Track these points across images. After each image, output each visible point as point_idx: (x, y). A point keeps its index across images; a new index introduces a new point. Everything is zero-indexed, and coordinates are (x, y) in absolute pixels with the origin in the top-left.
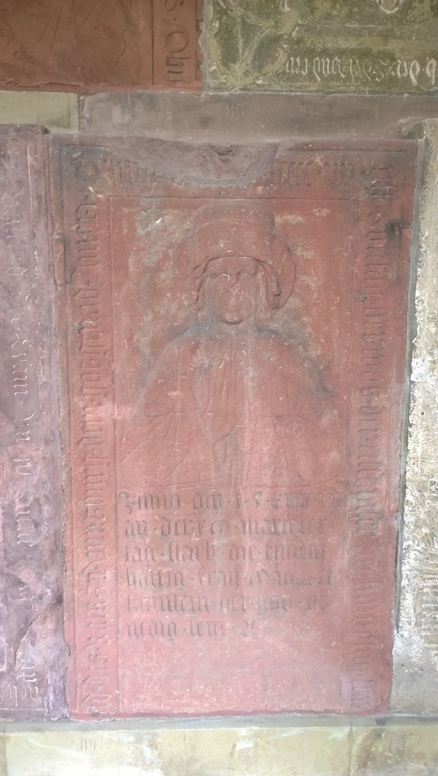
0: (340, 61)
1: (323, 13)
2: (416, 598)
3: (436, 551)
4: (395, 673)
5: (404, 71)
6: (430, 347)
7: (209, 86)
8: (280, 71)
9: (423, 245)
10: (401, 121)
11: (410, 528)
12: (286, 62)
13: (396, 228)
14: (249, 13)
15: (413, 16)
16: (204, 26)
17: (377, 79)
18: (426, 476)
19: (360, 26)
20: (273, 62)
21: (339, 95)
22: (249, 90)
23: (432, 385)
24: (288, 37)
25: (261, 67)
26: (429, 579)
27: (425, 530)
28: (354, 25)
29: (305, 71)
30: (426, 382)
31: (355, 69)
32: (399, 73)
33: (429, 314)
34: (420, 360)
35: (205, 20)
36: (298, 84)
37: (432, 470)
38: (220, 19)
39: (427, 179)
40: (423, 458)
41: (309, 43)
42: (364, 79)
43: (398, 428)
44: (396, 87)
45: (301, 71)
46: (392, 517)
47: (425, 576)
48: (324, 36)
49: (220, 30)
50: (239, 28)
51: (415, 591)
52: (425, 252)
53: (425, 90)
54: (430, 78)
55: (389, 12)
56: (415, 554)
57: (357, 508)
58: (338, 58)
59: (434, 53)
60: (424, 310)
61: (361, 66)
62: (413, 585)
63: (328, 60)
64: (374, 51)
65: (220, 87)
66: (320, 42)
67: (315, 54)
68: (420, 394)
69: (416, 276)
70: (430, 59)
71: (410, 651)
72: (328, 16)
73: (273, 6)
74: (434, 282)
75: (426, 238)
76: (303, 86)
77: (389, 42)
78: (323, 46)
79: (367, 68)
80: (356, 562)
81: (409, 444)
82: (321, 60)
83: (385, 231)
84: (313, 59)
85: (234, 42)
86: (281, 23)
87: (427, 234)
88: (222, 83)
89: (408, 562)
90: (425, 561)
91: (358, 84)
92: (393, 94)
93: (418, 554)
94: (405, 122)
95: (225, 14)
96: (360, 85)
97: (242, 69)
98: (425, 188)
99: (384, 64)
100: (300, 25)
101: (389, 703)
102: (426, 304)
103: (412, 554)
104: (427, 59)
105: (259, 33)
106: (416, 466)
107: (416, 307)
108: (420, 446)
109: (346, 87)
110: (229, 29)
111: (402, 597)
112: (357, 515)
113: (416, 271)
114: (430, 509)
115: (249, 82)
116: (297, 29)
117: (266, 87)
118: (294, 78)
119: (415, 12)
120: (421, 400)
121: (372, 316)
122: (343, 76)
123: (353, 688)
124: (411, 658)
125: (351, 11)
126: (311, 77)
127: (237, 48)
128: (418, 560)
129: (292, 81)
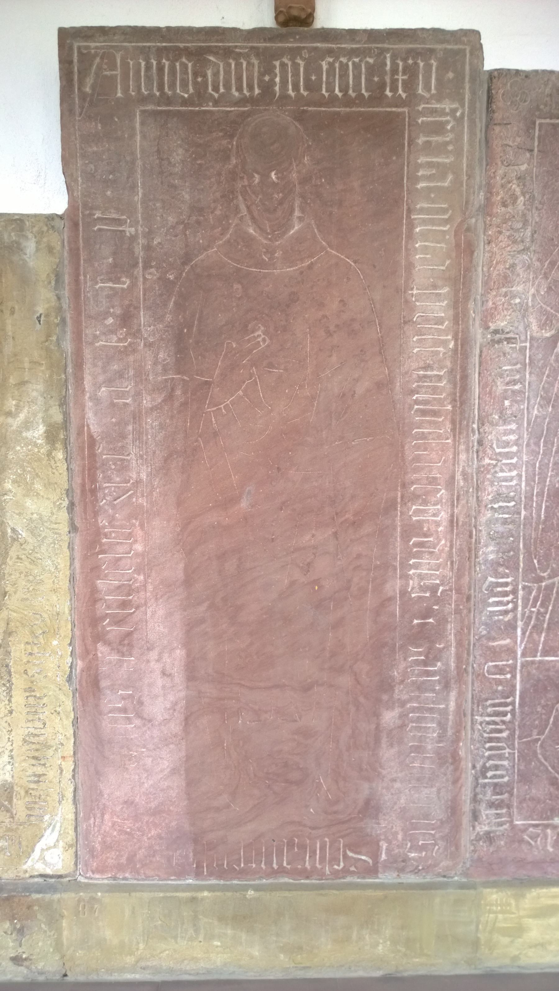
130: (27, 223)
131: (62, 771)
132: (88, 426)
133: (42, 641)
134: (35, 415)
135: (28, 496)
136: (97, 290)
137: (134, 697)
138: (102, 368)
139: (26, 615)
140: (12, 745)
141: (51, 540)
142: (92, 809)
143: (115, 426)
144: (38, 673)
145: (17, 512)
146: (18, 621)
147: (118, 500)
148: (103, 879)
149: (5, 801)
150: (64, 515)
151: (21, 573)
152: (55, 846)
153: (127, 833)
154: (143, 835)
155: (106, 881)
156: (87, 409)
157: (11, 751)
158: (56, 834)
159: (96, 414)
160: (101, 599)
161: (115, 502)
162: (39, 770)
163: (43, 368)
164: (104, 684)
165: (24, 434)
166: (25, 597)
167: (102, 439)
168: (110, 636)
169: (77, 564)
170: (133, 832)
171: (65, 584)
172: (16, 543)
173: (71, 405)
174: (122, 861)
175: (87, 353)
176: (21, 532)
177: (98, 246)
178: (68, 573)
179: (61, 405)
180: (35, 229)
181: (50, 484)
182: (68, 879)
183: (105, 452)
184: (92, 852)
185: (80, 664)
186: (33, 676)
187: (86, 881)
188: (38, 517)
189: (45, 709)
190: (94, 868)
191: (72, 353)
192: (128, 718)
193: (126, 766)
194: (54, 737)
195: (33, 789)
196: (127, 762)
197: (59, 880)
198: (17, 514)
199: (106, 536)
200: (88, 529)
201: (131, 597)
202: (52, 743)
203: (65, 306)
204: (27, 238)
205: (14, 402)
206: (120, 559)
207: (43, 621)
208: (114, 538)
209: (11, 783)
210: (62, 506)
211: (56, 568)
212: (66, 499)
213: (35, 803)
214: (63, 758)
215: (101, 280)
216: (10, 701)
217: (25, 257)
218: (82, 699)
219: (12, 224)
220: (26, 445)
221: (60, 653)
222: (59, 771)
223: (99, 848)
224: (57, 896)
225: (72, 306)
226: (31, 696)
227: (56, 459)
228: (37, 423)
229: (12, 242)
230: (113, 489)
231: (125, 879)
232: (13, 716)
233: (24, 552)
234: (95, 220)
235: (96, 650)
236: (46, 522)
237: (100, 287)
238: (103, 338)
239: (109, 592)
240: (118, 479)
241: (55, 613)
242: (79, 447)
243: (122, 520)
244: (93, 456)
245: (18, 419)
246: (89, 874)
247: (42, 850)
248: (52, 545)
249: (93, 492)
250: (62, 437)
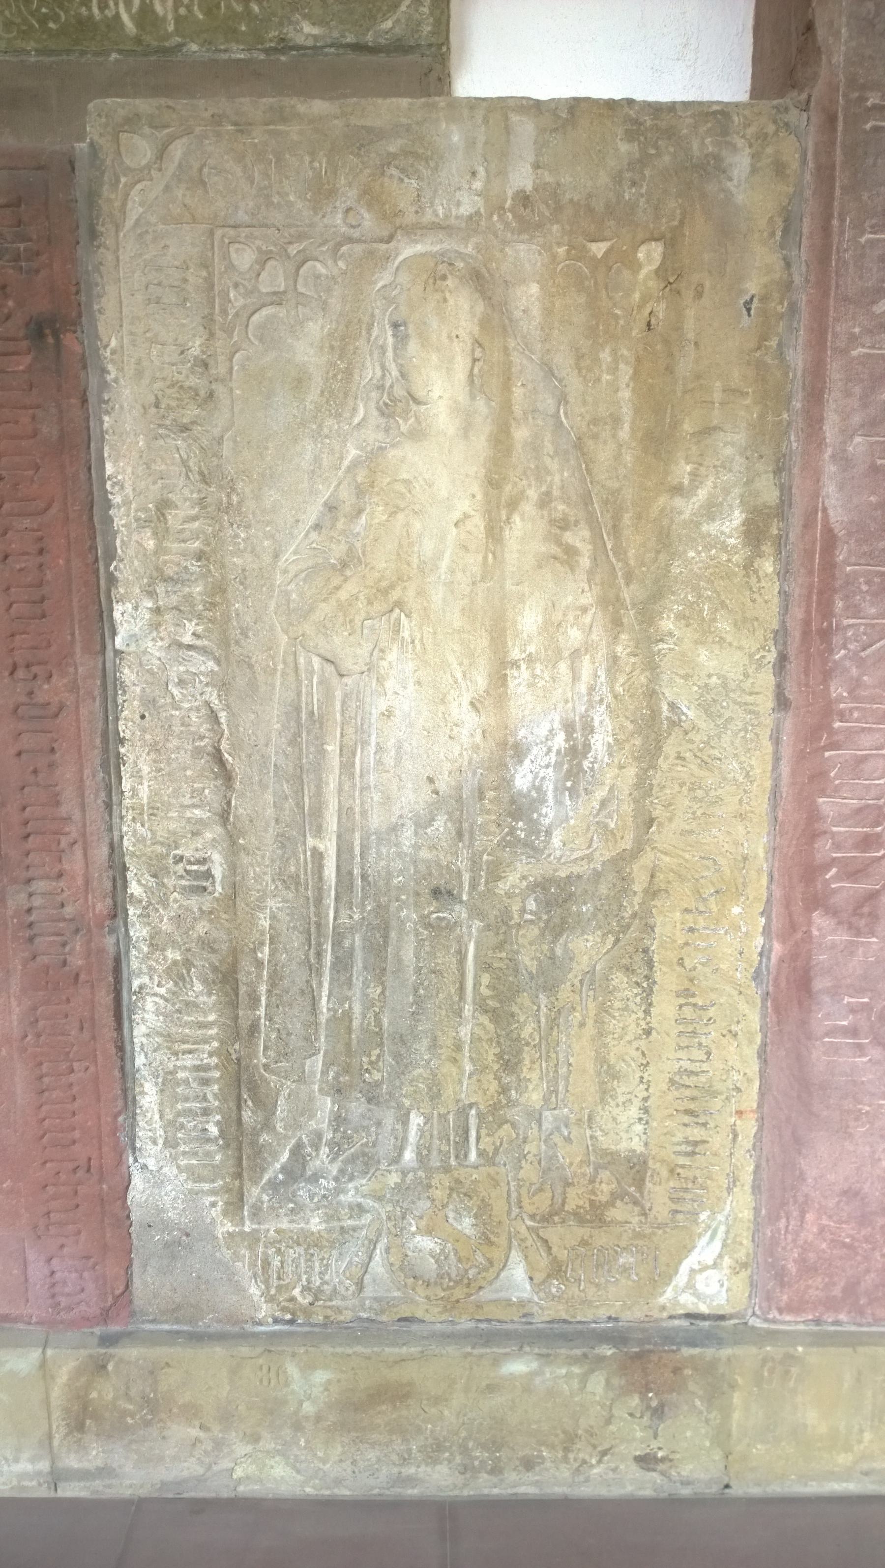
2: (162, 1091)
3: (197, 997)
4: (135, 1242)
6: (145, 581)
9: (110, 367)
11: (139, 950)
13: (47, 331)
17: (51, 25)
18: (162, 844)
23: (160, 659)
26: (184, 1053)
27: (172, 955)
30: (145, 652)
32: (96, 11)
33: (136, 511)
34: (129, 606)
37: (175, 833)
39: (100, 228)
40: (153, 808)
43: (94, 747)
46: (103, 927)
47: (176, 1047)
51: (158, 1076)
52: (116, 380)
53: (155, 44)
54: (164, 19)
56: (156, 1003)
57: (29, 911)
60: (127, 503)
62: (154, 1064)
68: (133, 677)
69: (102, 431)
71: (161, 1196)
74: (141, 443)
75: (114, 352)
80: (37, 1021)
81: (124, 781)
83: (26, 337)
87: (113, 343)
89: (143, 1019)
90: (176, 1016)
91: (11, 36)
93: (161, 1002)
96: (15, 38)
98: (98, 247)
101: (131, 1301)
102: (129, 490)
103: (150, 1004)
106: (139, 824)
107: (110, 497)
108: (146, 784)
111: (137, 1090)
112: (30, 925)
113: (102, 422)
114: (180, 912)
120: (138, 689)
121: (19, 515)
123: (53, 1273)
124: (162, 1211)
128: (162, 1014)
130: (736, 119)
131: (735, 1136)
132: (825, 510)
133: (715, 908)
134: (726, 491)
135: (702, 643)
136: (863, 247)
137: (872, 1009)
138: (861, 398)
139: (687, 861)
140: (647, 1090)
141: (740, 725)
142: (784, 1204)
143: (876, 509)
144: (703, 964)
145: (682, 672)
146: (672, 870)
147: (869, 651)
148: (797, 1323)
149: (630, 1186)
150: (767, 679)
151: (682, 785)
152: (715, 1265)
153: (844, 1245)
154: (873, 1249)
155: (801, 1327)
156: (825, 479)
157: (645, 1099)
158: (717, 1245)
159: (841, 488)
160: (825, 832)
161: (863, 654)
162: (696, 1133)
163: (748, 401)
164: (820, 984)
165: (705, 528)
166: (687, 827)
167: (849, 534)
168: (837, 900)
169: (785, 769)
170: (856, 1244)
171: (761, 805)
172: (676, 729)
173: (796, 471)
174: (834, 1293)
175: (835, 371)
176: (685, 710)
177: (870, 161)
178: (768, 784)
179: (778, 472)
180: (750, 131)
181: (745, 620)
182: (732, 1322)
183: (853, 560)
184: (781, 1277)
185: (777, 948)
186: (695, 969)
187: (765, 1325)
188: (719, 682)
189: (711, 1028)
190: (782, 1304)
191: (804, 370)
192: (859, 1046)
193: (849, 1130)
194: (724, 1077)
195: (683, 1167)
196: (852, 1123)
197: (718, 1323)
198: (682, 677)
199: (842, 718)
200: (811, 704)
201: (879, 829)
202: (718, 1086)
203: (797, 279)
204: (734, 148)
205: (688, 468)
206: (865, 758)
207: (717, 871)
208: (857, 721)
209: (642, 1154)
210: (766, 661)
211: (747, 775)
212: (773, 649)
213: (686, 1190)
214: (740, 1113)
215: (872, 227)
216: (647, 1012)
217: (729, 184)
218: (777, 1010)
219: (707, 122)
220: (708, 547)
221: (744, 929)
222: (731, 1136)
223: (794, 1270)
224: (726, 1352)
225: (812, 278)
226: (687, 1004)
227: (761, 573)
228: (730, 506)
229: (707, 155)
230: (862, 628)
231: (837, 1323)
232: (651, 1038)
233: (691, 746)
234: (870, 109)
235: (810, 923)
236: (734, 691)
237: (869, 241)
238: (867, 340)
239: (841, 819)
240: (873, 611)
241: (740, 858)
242: (805, 550)
243: (874, 687)
244: (829, 566)
245: (695, 499)
246: (774, 1314)
247: (693, 1271)
248: (742, 734)
249: (825, 635)
250: (776, 532)
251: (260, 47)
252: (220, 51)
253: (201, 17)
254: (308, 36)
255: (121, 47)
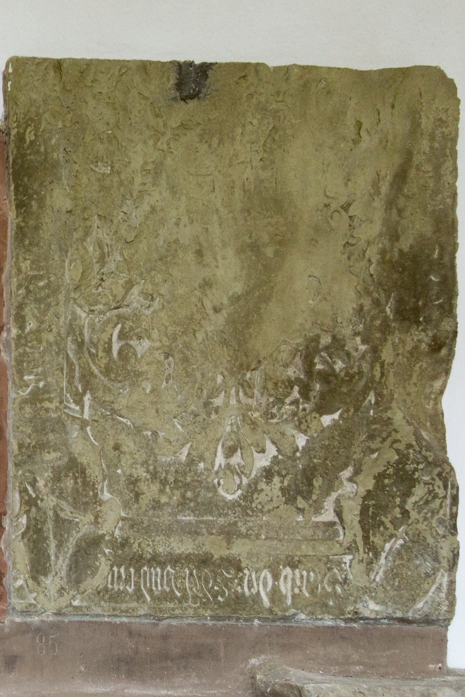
0: (173, 571)
1: (150, 500)
5: (252, 586)
7: (14, 609)
8: (101, 587)
10: (254, 661)
12: (109, 573)
14: (62, 502)
15: (260, 503)
16: (8, 521)
17: (220, 598)
19: (196, 518)
20: (93, 574)
21: (174, 622)
22: (64, 614)
24: (110, 538)
25: (78, 582)
28: (188, 518)
29: (130, 587)
31: (192, 584)
32: (246, 589)
35: (9, 512)
36: (124, 606)
38: (28, 512)
41: (136, 545)
42: (204, 598)
44: (244, 609)
45: (126, 585)
48: (154, 534)
49: (28, 528)
50: (50, 525)
53: (280, 613)
54: (286, 597)
55: (229, 497)
58: (171, 568)
59: (289, 559)
61: (200, 578)
63: (159, 570)
64: (216, 557)
65: (28, 610)
66: (149, 545)
67: (143, 561)
70: (284, 567)
72: (157, 505)
73: (91, 493)
76: (130, 608)
77: (233, 543)
78: (153, 551)
79: (207, 582)
82: (150, 571)
84: (141, 568)
85: (45, 545)
86: (101, 518)
88: (30, 605)
91: (196, 606)
92: (240, 619)
94: (257, 664)
95: (35, 506)
96: (199, 608)
97: (56, 585)
99: (228, 576)
100: (123, 519)
104: (281, 567)
105: (74, 532)
109: (182, 610)
110: (39, 527)
115: (65, 604)
116: (120, 525)
117: (84, 610)
118: (118, 596)
119: (262, 497)
122: (179, 594)
125: (183, 496)
126: (138, 595)
127: (48, 554)
129: (116, 602)
251: (342, 617)
252: (317, 619)
253: (307, 595)
254: (372, 611)
255: (260, 616)
